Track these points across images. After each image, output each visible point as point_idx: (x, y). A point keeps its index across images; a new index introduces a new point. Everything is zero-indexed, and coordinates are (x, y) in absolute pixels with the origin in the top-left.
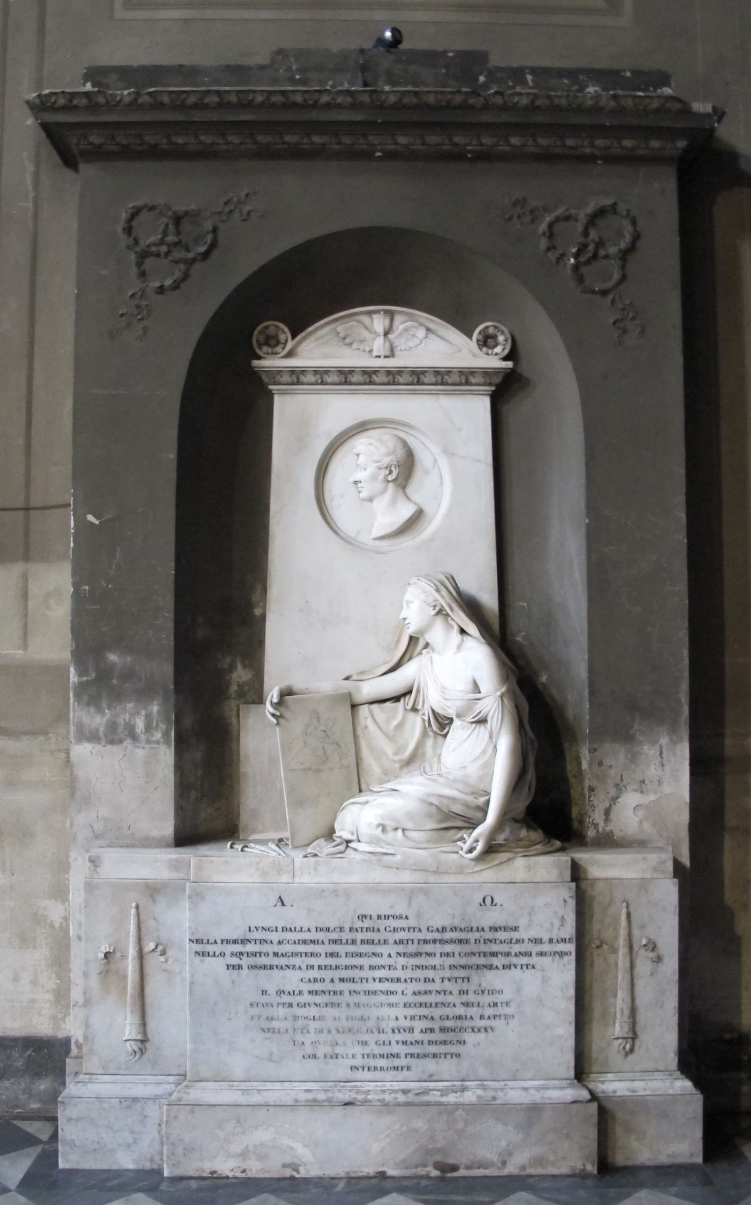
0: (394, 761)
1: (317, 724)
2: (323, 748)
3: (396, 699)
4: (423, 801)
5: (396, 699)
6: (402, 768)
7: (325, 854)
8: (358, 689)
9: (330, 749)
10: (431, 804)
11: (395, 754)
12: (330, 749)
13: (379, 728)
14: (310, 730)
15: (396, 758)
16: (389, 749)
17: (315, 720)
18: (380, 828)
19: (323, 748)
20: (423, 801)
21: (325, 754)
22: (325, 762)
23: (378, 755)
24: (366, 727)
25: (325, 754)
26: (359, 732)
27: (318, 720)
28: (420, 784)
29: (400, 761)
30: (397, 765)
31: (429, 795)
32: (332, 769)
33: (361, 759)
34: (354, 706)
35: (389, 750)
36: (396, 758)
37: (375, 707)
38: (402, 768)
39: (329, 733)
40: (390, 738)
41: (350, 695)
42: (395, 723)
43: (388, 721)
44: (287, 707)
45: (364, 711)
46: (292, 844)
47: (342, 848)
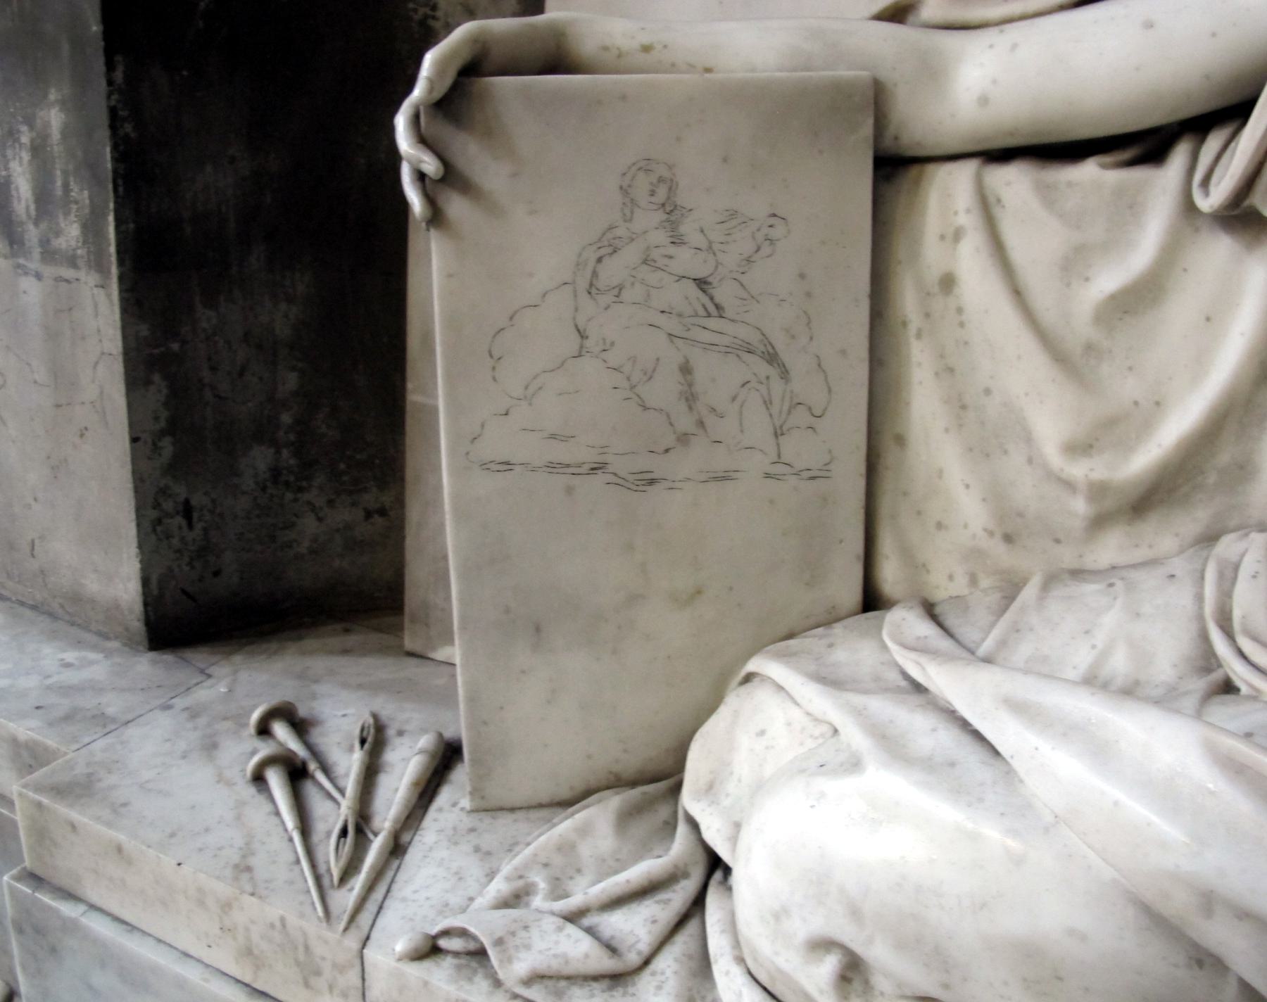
0: (1069, 485)
1: (660, 237)
2: (686, 369)
3: (1146, 145)
4: (1157, 922)
5: (1146, 145)
6: (1099, 523)
7: (522, 966)
8: (933, 72)
9: (721, 377)
10: (1206, 961)
11: (1079, 448)
12: (721, 377)
13: (1018, 293)
14: (613, 271)
15: (1079, 470)
16: (1050, 419)
17: (648, 220)
18: (829, 965)
19: (686, 369)
20: (1157, 922)
21: (690, 398)
22: (684, 439)
23: (991, 435)
24: (948, 283)
25: (690, 398)
26: (908, 301)
27: (672, 211)
28: (1165, 793)
29: (1098, 491)
30: (1080, 506)
31: (1209, 901)
32: (724, 477)
33: (900, 440)
34: (895, 166)
35: (1050, 419)
36: (1079, 470)
37: (1013, 182)
38: (1099, 523)
39: (724, 293)
40: (1068, 360)
41: (878, 98)
42: (1109, 280)
43: (1074, 264)
44: (491, 134)
45: (949, 193)
46: (476, 792)
47: (636, 926)
